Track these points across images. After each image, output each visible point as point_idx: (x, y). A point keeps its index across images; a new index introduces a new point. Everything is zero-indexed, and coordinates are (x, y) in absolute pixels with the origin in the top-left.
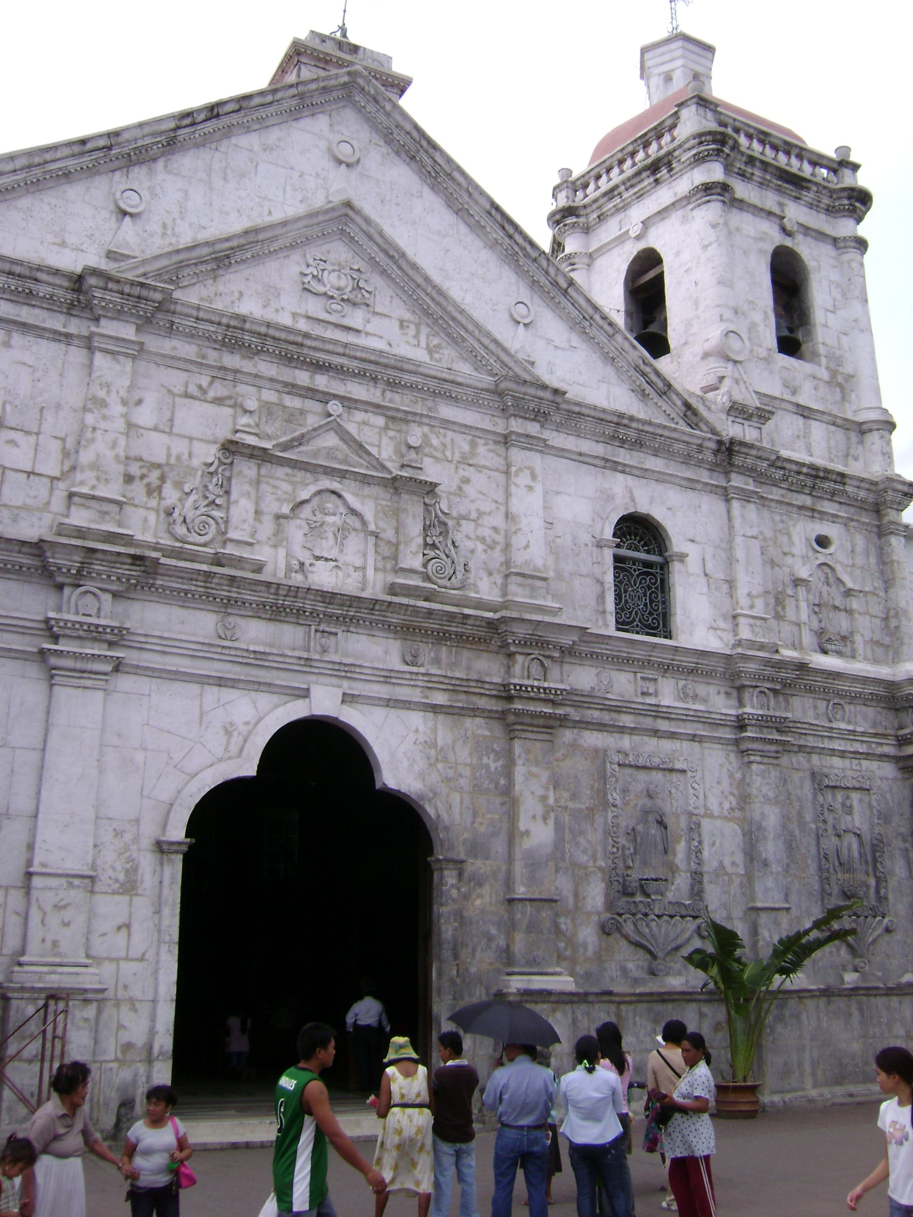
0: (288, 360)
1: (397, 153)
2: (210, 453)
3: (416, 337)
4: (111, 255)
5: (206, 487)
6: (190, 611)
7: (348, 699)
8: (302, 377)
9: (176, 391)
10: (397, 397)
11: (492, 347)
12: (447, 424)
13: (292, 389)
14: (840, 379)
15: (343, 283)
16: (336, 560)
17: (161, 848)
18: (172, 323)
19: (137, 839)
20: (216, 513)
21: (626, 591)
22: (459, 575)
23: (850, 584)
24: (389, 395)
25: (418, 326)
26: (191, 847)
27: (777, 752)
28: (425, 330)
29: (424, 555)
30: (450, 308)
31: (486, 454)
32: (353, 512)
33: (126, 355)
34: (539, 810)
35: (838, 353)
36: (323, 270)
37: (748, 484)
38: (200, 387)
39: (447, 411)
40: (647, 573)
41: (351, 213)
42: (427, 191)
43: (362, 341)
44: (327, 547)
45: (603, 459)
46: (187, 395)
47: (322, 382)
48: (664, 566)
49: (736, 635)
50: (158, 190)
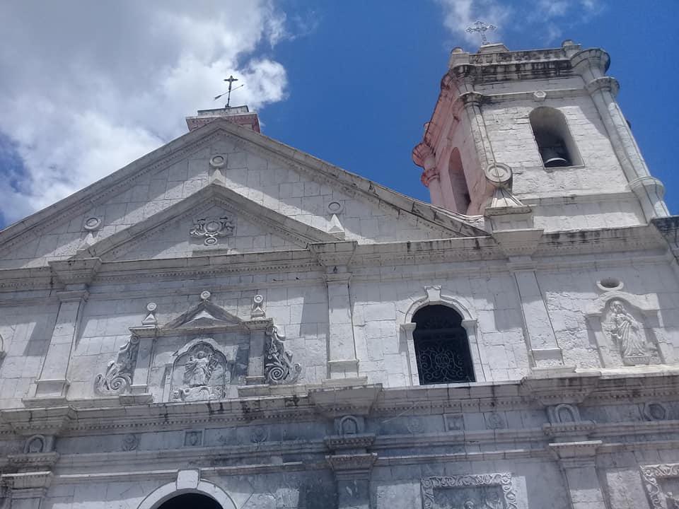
29: (265, 367)
32: (216, 352)
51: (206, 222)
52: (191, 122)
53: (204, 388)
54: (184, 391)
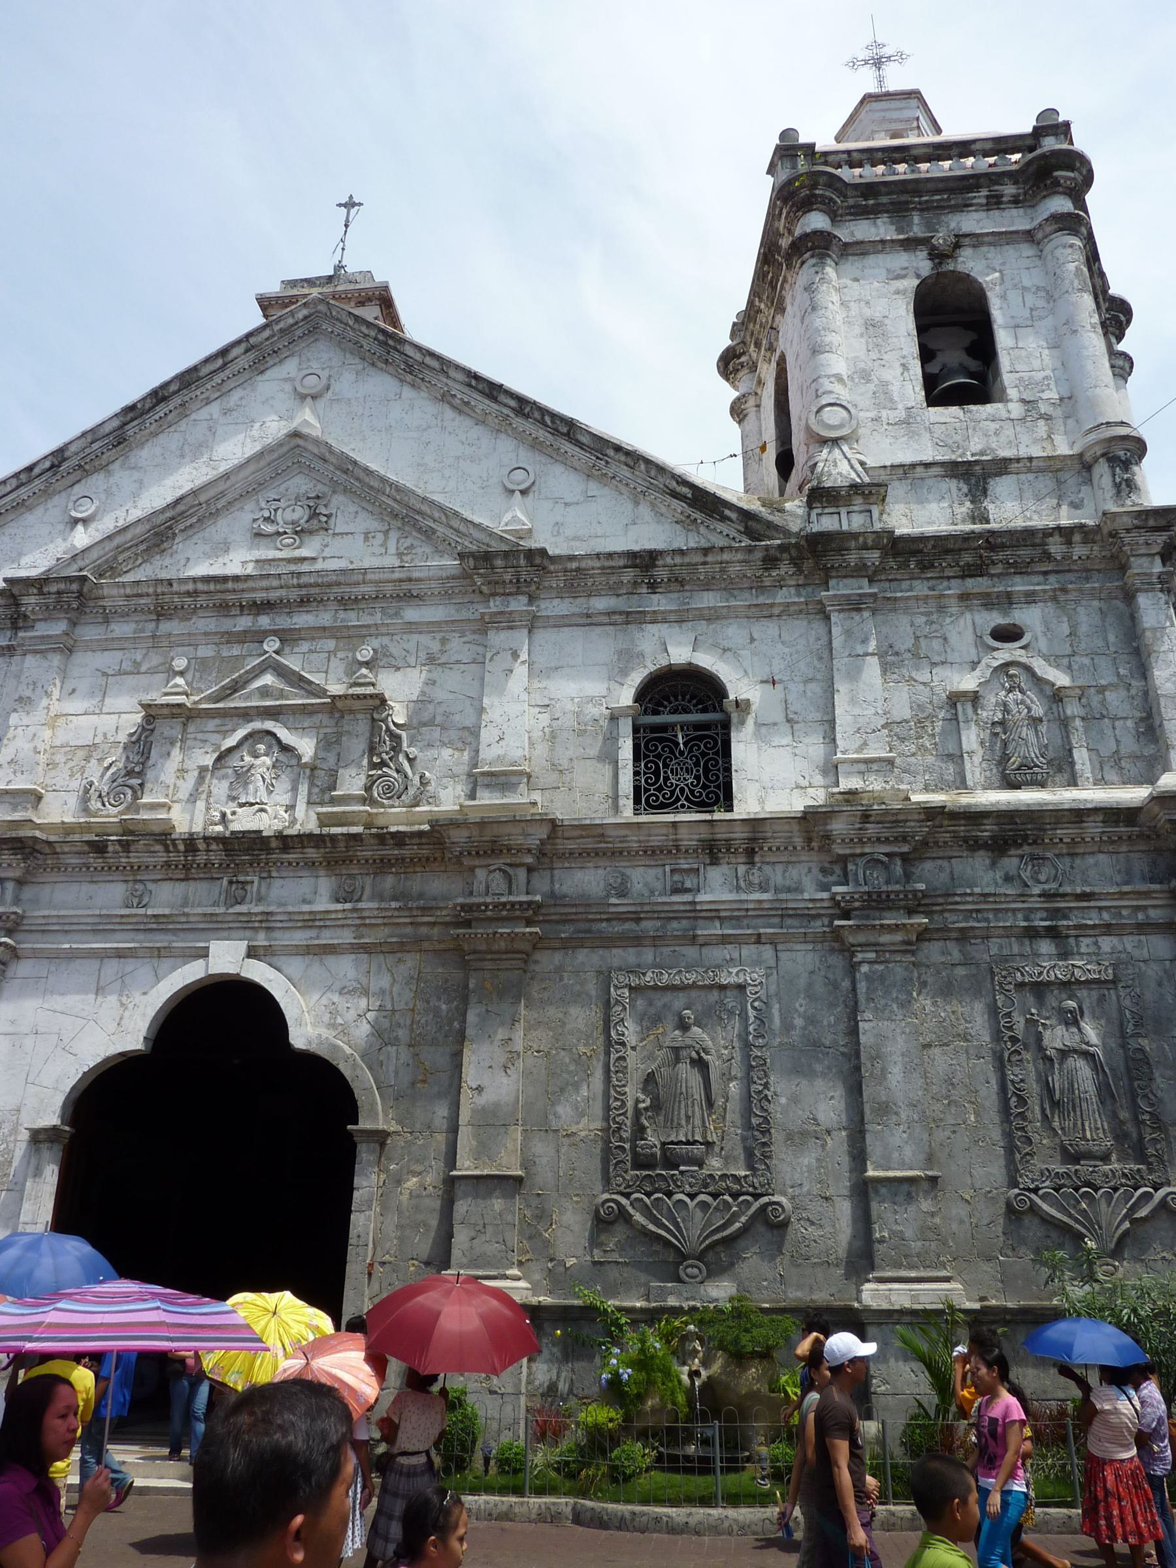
0: (223, 608)
1: (373, 364)
3: (384, 544)
6: (103, 885)
7: (252, 953)
8: (244, 623)
9: (110, 672)
10: (352, 615)
11: (462, 528)
12: (412, 628)
13: (231, 638)
14: (1043, 408)
15: (296, 516)
16: (263, 803)
18: (104, 608)
20: (135, 782)
21: (666, 766)
22: (412, 791)
24: (342, 614)
25: (386, 533)
27: (905, 943)
28: (394, 536)
30: (412, 502)
31: (459, 648)
32: (286, 748)
33: (54, 650)
36: (275, 510)
37: (860, 588)
38: (135, 662)
39: (412, 614)
40: (700, 738)
41: (300, 442)
42: (408, 392)
43: (319, 565)
45: (621, 613)
46: (120, 673)
47: (264, 621)
48: (726, 726)
50: (114, 489)
51: (282, 504)
52: (266, 303)
53: (262, 810)
54: (228, 812)
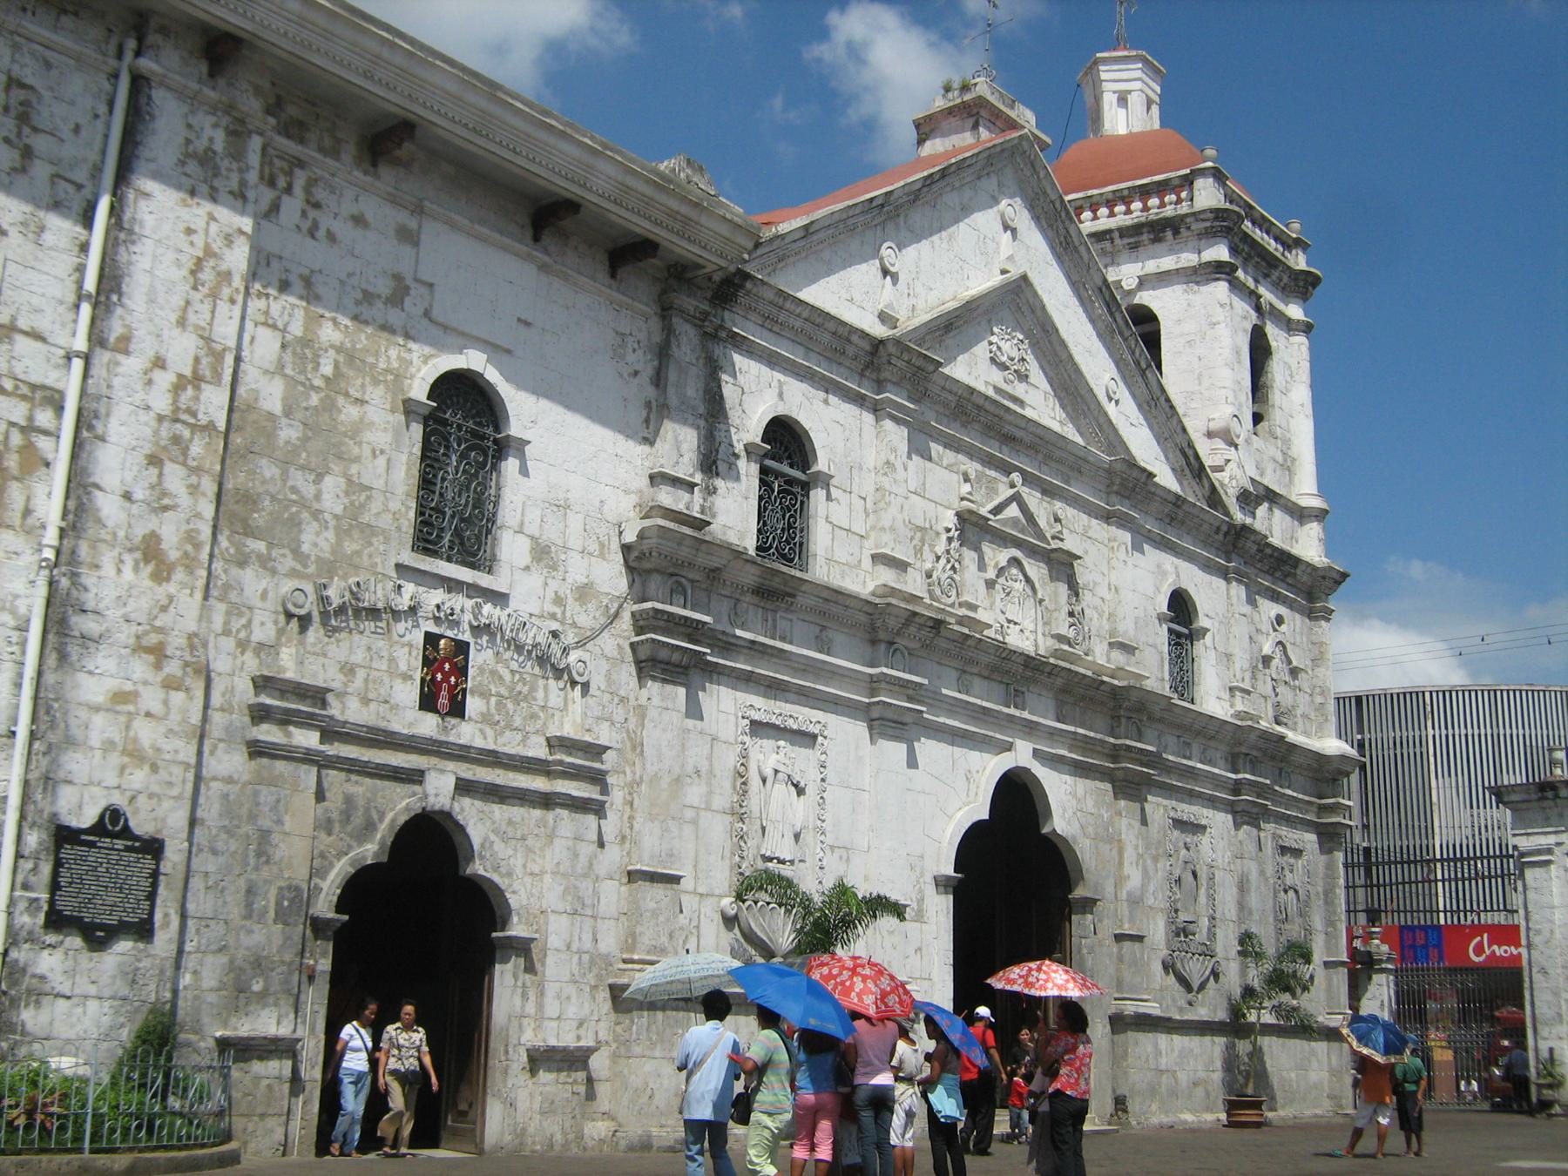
2: (950, 520)
4: (884, 317)
5: (948, 552)
17: (941, 883)
19: (922, 874)
23: (1295, 663)
26: (960, 881)
32: (1028, 580)
34: (1134, 859)
35: (1288, 435)
44: (1013, 612)
49: (1232, 706)
